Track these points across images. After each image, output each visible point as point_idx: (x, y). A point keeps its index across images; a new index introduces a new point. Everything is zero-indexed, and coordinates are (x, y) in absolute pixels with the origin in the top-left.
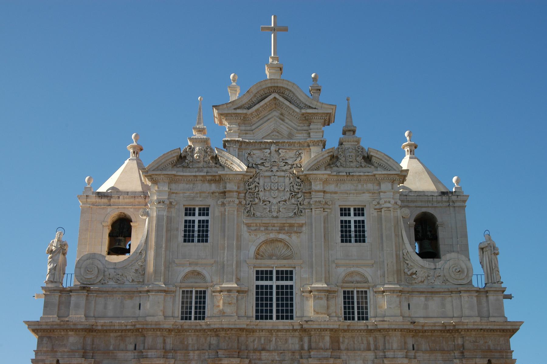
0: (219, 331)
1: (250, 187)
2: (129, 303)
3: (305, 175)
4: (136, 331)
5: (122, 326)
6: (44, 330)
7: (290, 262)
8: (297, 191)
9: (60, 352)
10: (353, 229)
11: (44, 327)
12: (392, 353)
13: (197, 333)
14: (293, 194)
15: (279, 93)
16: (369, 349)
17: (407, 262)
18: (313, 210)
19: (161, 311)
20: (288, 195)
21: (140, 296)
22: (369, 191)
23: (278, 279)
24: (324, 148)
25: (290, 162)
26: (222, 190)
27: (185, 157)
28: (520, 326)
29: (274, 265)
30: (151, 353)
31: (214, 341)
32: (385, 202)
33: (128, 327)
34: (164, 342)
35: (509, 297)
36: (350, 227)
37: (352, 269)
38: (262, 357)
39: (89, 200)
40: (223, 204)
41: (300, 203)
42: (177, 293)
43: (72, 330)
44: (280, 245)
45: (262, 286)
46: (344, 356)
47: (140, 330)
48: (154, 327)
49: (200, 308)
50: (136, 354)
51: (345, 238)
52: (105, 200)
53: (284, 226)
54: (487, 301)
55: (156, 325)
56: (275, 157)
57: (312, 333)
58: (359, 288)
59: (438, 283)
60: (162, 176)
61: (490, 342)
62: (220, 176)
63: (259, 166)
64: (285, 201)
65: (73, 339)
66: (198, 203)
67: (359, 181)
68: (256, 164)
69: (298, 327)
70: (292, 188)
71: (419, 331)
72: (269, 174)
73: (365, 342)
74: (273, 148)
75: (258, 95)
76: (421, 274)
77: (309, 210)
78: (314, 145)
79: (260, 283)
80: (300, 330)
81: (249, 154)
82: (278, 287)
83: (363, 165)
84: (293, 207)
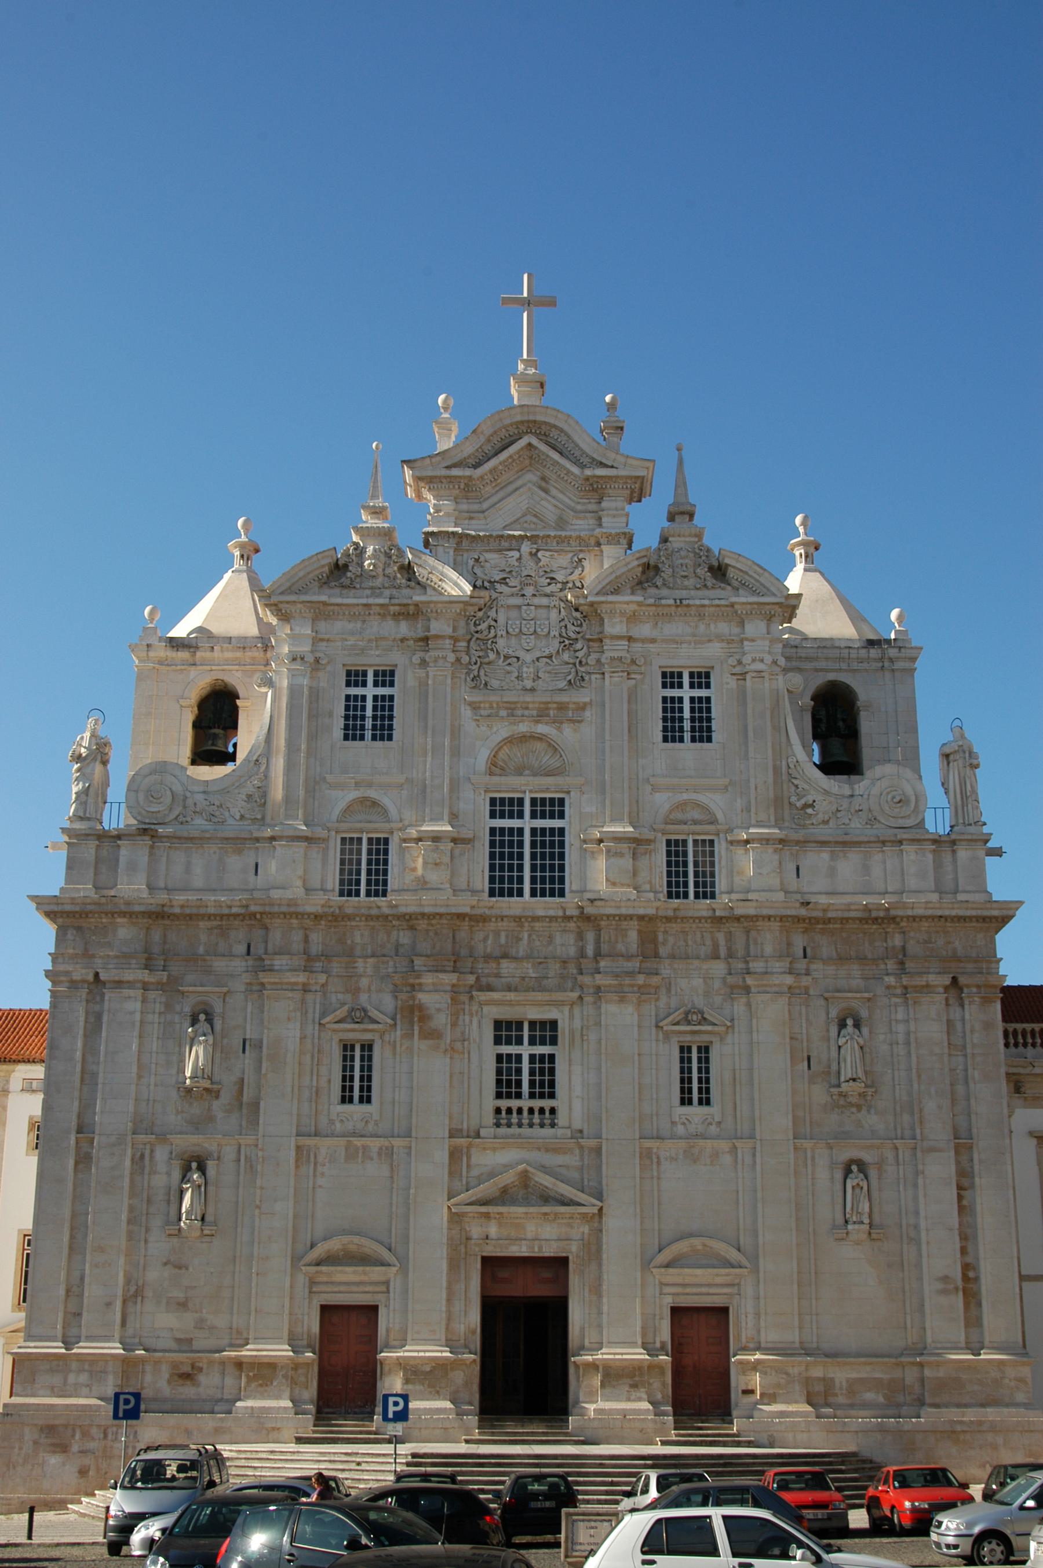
0: (417, 919)
1: (479, 628)
2: (235, 863)
3: (592, 604)
4: (250, 919)
5: (221, 906)
6: (68, 914)
7: (559, 780)
8: (573, 636)
10: (687, 714)
11: (68, 908)
12: (762, 964)
13: (371, 923)
14: (567, 643)
15: (537, 435)
16: (716, 957)
17: (796, 782)
18: (607, 676)
19: (300, 877)
20: (555, 645)
21: (257, 848)
22: (720, 638)
23: (534, 815)
24: (630, 548)
25: (560, 577)
26: (421, 634)
27: (346, 566)
28: (1017, 909)
29: (527, 788)
30: (279, 962)
31: (405, 938)
32: (754, 660)
33: (234, 910)
34: (306, 940)
35: (998, 852)
36: (681, 710)
37: (685, 796)
38: (502, 971)
39: (151, 654)
40: (424, 663)
41: (580, 662)
42: (332, 844)
43: (123, 914)
44: (539, 746)
45: (502, 830)
46: (666, 971)
47: (258, 916)
48: (284, 909)
49: (377, 871)
50: (250, 963)
51: (672, 733)
52: (184, 655)
53: (548, 709)
54: (955, 860)
56: (530, 567)
57: (603, 923)
58: (699, 834)
59: (856, 824)
60: (299, 606)
61: (957, 943)
62: (417, 605)
63: (497, 586)
64: (550, 657)
65: (125, 932)
66: (373, 661)
67: (701, 616)
68: (490, 582)
69: (572, 912)
70: (563, 630)
71: (817, 921)
72: (517, 601)
73: (708, 942)
74: (526, 548)
75: (495, 439)
76: (824, 807)
77: (598, 676)
78: (609, 543)
79: (499, 823)
80: (578, 917)
81: (477, 560)
82: (534, 831)
83: (709, 584)
84: (565, 669)
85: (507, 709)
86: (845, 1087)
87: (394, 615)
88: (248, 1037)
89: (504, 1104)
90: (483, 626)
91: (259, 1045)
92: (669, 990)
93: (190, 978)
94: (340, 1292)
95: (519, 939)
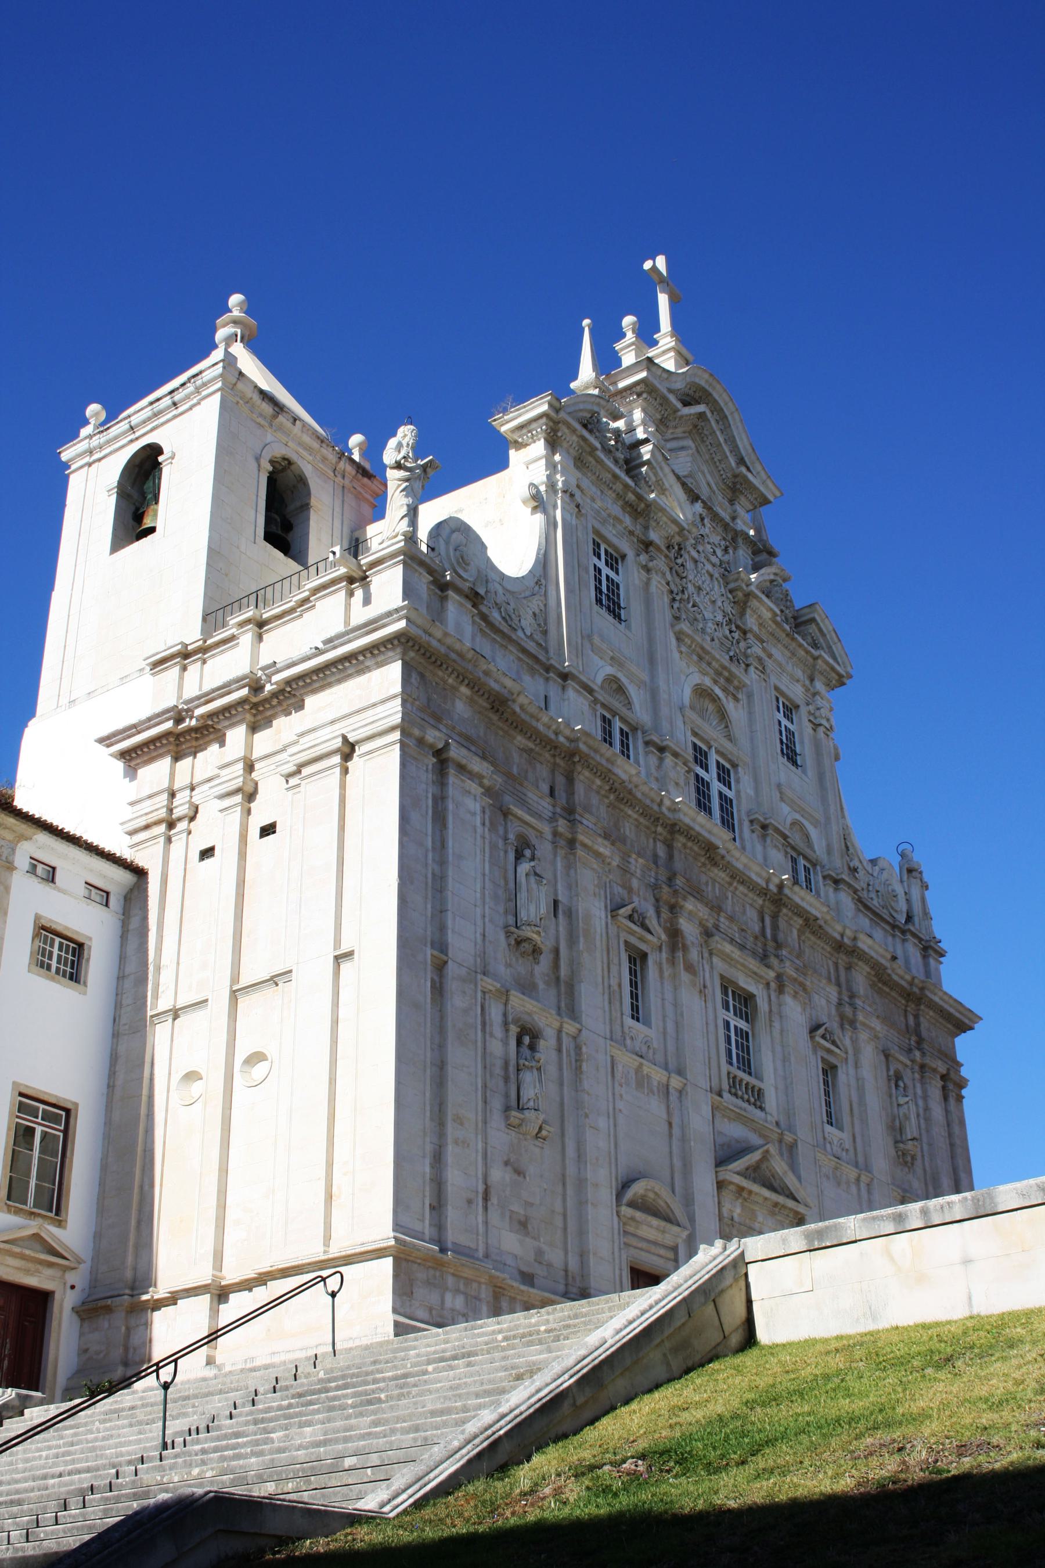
5: (549, 727)
9: (446, 726)
37: (798, 817)
44: (711, 707)
55: (608, 760)
60: (575, 438)
86: (910, 1145)
87: (627, 503)
88: (560, 898)
91: (570, 914)
94: (641, 1249)
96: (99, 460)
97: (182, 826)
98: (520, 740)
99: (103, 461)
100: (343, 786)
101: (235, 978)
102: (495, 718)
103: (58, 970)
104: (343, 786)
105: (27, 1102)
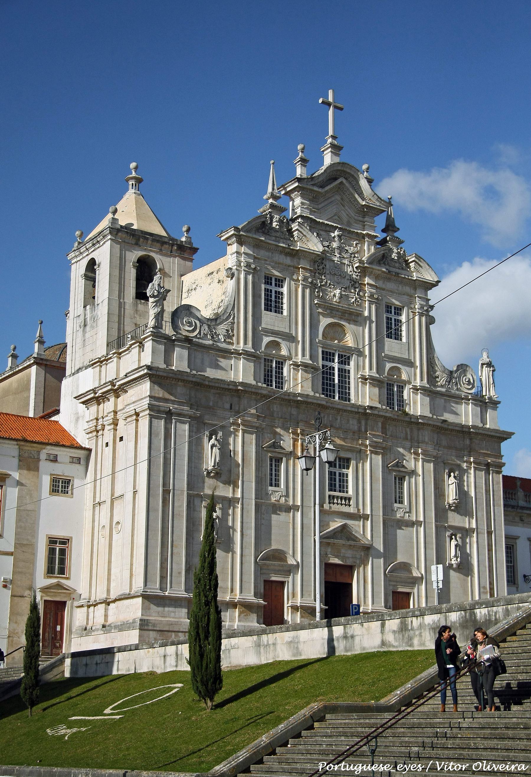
15: (346, 179)
48: (253, 390)
53: (346, 313)
60: (250, 239)
73: (404, 432)
80: (362, 413)
85: (330, 309)
89: (333, 493)
90: (321, 267)
92: (390, 452)
93: (207, 417)
95: (337, 419)
96: (79, 261)
97: (100, 433)
98: (213, 391)
99: (81, 261)
100: (137, 427)
101: (112, 495)
102: (199, 388)
103: (62, 491)
104: (137, 427)
105: (52, 541)
